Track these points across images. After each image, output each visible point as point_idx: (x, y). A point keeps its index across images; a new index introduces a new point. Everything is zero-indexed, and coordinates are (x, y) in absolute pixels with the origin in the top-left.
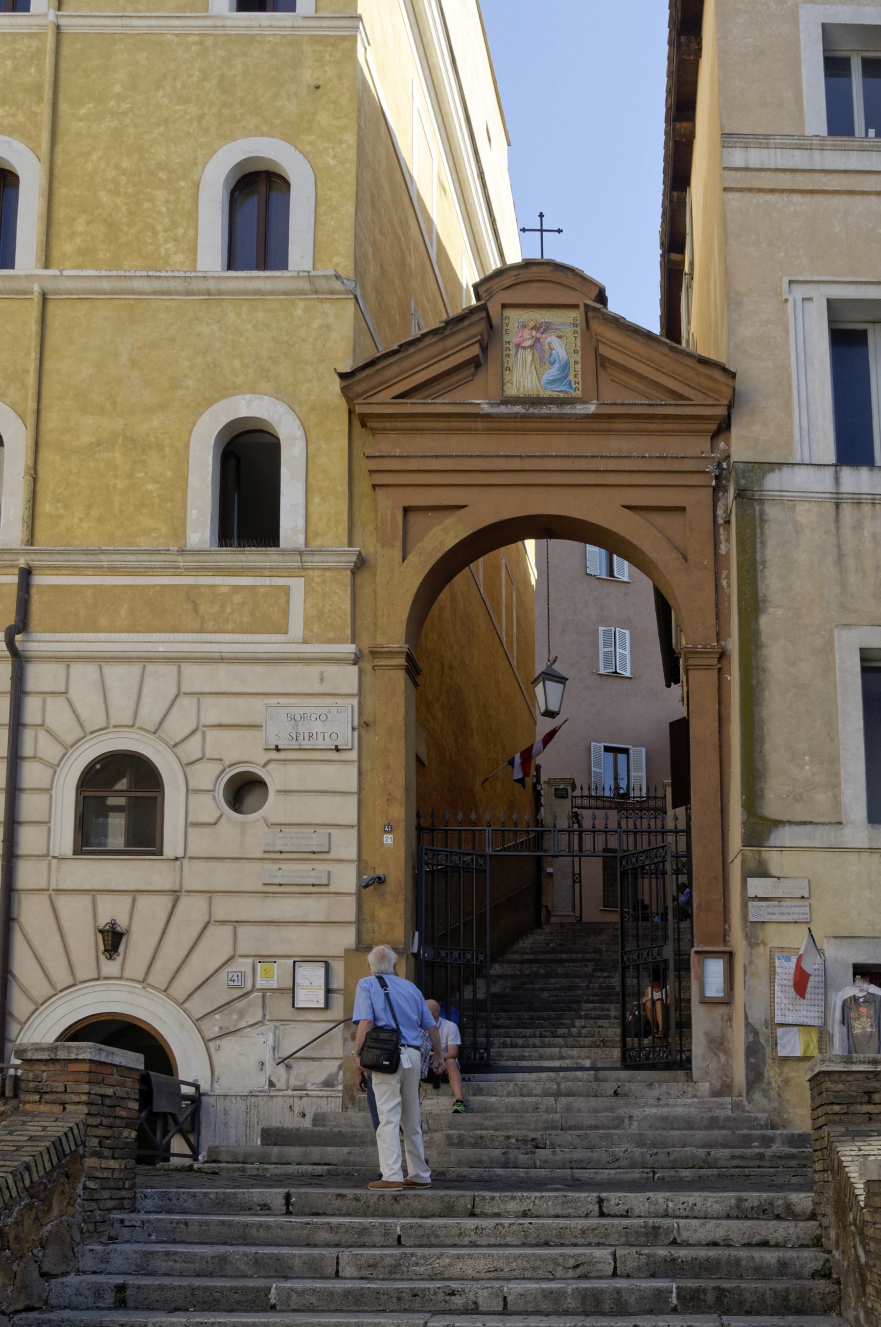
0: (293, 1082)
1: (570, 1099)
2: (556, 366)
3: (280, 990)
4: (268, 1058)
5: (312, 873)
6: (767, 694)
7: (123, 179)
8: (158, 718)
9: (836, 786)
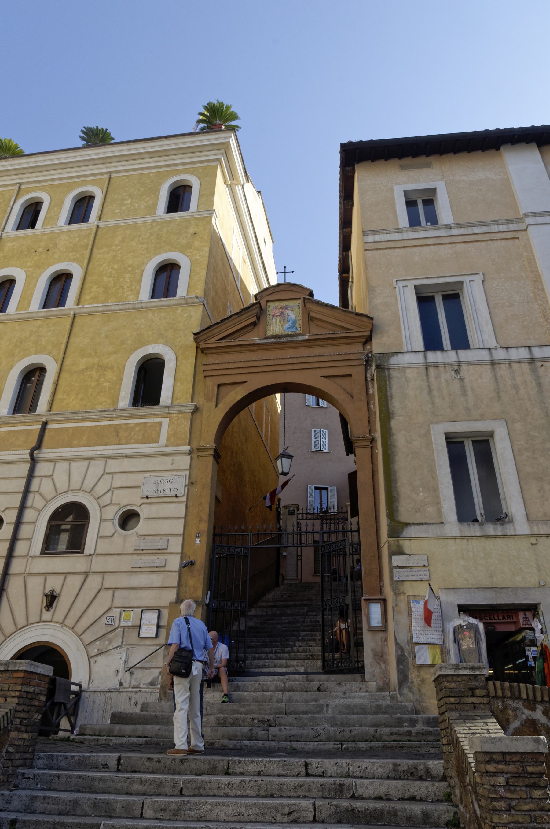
0: (133, 683)
1: (291, 693)
2: (291, 322)
3: (133, 627)
4: (121, 667)
5: (157, 561)
6: (397, 458)
7: (114, 272)
9: (438, 503)
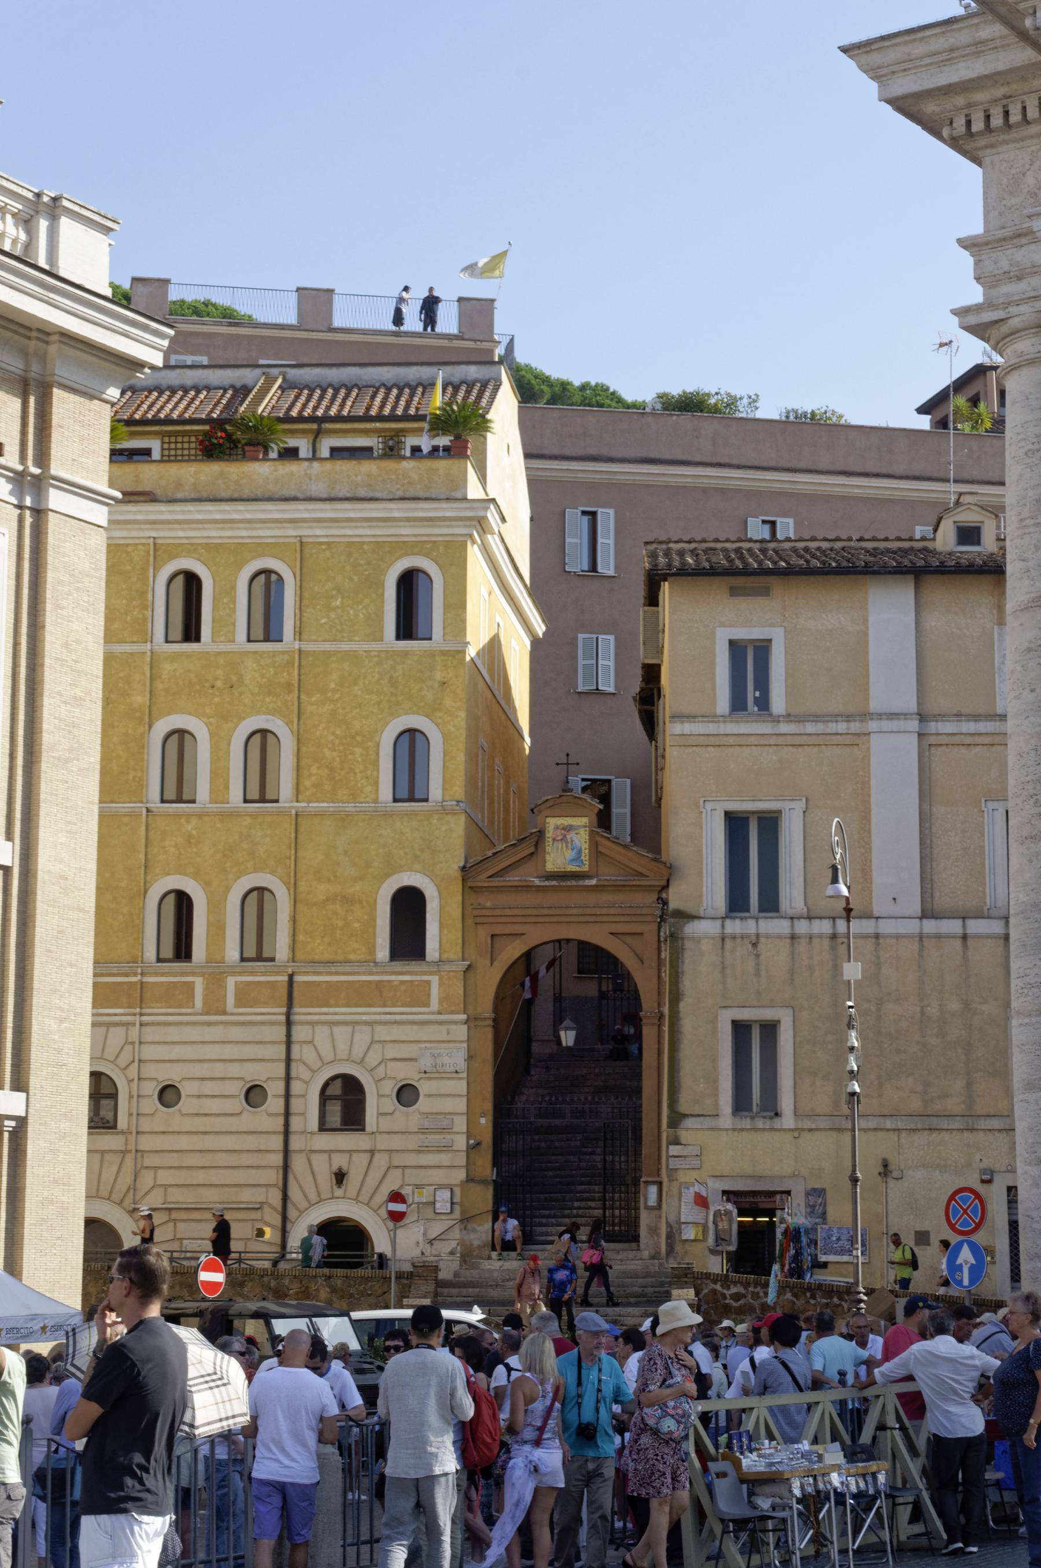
0: (434, 1252)
3: (427, 1203)
4: (421, 1239)
7: (337, 741)
8: (362, 1055)
